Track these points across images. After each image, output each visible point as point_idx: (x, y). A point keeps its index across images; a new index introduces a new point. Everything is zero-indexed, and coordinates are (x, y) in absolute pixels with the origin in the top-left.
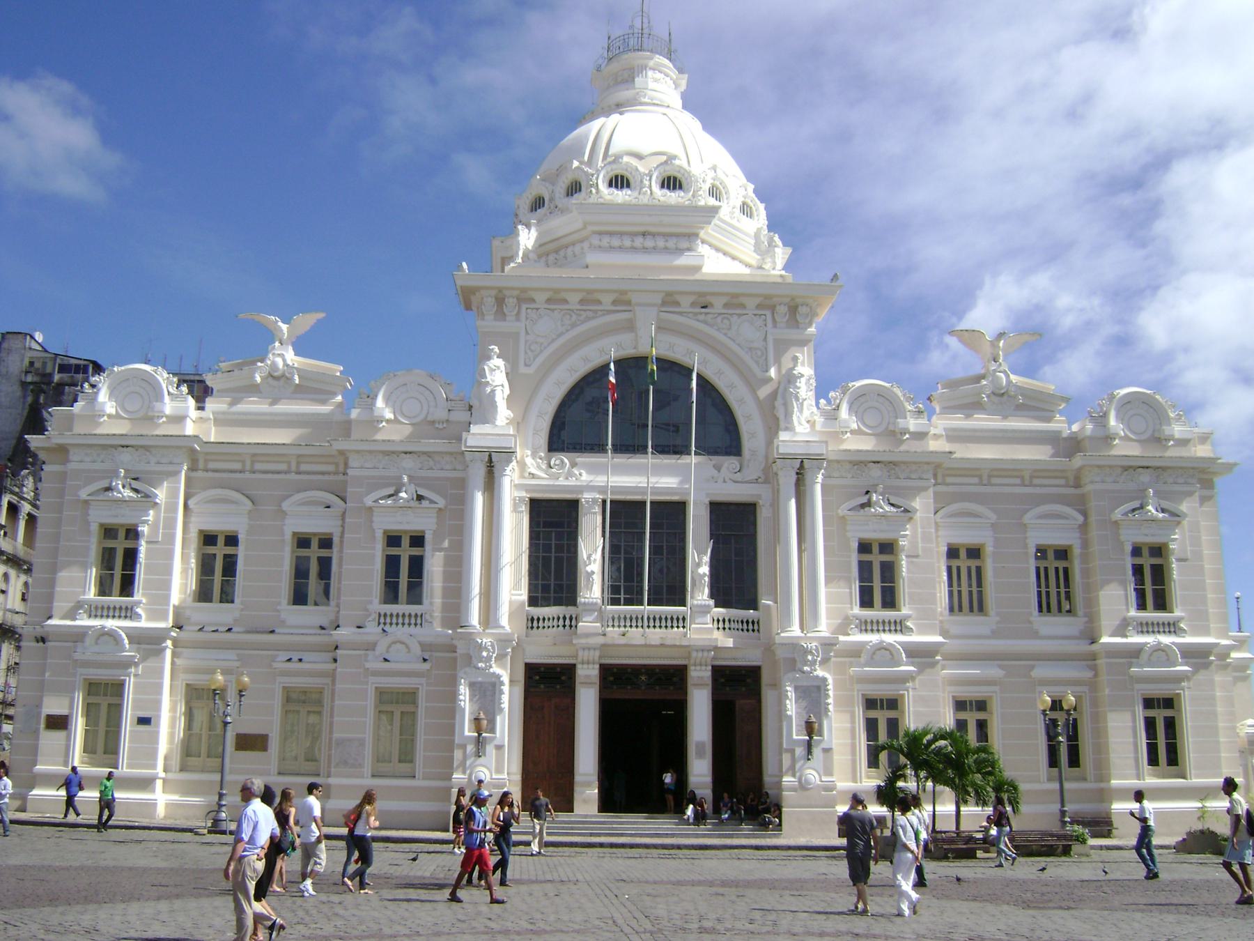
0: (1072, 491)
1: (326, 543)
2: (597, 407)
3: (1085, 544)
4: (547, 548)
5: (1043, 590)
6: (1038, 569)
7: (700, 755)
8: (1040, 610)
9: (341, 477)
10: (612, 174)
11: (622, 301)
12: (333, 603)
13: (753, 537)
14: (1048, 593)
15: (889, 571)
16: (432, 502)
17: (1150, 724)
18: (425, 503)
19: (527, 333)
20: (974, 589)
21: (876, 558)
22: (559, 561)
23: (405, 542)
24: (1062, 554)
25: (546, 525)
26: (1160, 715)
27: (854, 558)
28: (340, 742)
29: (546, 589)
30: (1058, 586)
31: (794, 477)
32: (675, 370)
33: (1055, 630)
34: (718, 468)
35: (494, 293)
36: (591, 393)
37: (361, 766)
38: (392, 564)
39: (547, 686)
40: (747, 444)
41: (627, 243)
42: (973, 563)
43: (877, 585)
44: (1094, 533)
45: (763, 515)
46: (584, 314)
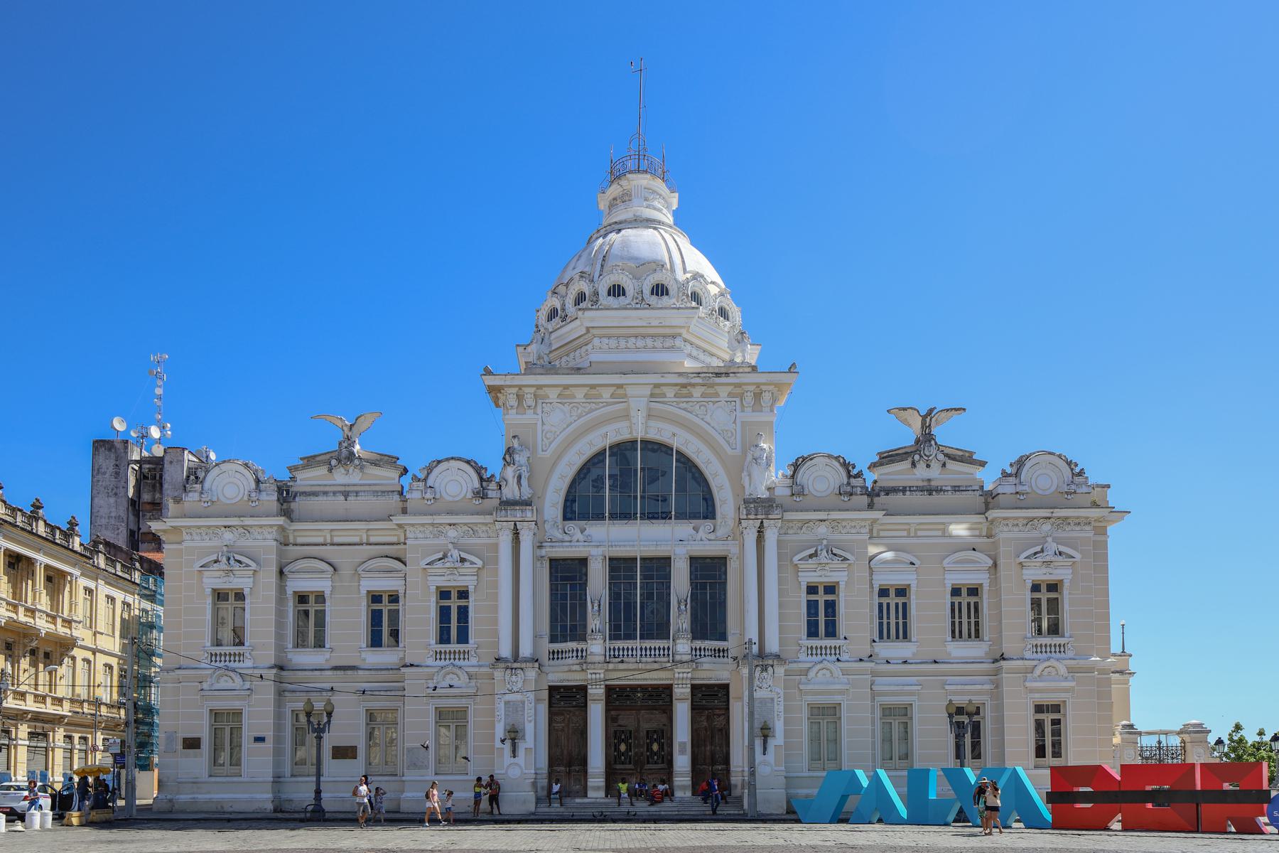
0: (986, 540)
1: (394, 598)
2: (599, 482)
3: (995, 580)
4: (564, 597)
5: (957, 620)
7: (682, 752)
8: (953, 637)
9: (402, 546)
13: (724, 584)
14: (960, 623)
15: (831, 607)
16: (472, 563)
17: (1039, 726)
18: (467, 565)
19: (543, 424)
20: (901, 621)
21: (821, 598)
22: (573, 607)
23: (454, 595)
24: (974, 591)
25: (563, 578)
26: (1048, 718)
27: (804, 598)
29: (564, 628)
30: (969, 617)
34: (696, 529)
35: (515, 390)
36: (595, 472)
37: (427, 767)
38: (444, 613)
39: (565, 702)
41: (623, 343)
42: (900, 600)
43: (822, 618)
45: (732, 567)
46: (589, 406)
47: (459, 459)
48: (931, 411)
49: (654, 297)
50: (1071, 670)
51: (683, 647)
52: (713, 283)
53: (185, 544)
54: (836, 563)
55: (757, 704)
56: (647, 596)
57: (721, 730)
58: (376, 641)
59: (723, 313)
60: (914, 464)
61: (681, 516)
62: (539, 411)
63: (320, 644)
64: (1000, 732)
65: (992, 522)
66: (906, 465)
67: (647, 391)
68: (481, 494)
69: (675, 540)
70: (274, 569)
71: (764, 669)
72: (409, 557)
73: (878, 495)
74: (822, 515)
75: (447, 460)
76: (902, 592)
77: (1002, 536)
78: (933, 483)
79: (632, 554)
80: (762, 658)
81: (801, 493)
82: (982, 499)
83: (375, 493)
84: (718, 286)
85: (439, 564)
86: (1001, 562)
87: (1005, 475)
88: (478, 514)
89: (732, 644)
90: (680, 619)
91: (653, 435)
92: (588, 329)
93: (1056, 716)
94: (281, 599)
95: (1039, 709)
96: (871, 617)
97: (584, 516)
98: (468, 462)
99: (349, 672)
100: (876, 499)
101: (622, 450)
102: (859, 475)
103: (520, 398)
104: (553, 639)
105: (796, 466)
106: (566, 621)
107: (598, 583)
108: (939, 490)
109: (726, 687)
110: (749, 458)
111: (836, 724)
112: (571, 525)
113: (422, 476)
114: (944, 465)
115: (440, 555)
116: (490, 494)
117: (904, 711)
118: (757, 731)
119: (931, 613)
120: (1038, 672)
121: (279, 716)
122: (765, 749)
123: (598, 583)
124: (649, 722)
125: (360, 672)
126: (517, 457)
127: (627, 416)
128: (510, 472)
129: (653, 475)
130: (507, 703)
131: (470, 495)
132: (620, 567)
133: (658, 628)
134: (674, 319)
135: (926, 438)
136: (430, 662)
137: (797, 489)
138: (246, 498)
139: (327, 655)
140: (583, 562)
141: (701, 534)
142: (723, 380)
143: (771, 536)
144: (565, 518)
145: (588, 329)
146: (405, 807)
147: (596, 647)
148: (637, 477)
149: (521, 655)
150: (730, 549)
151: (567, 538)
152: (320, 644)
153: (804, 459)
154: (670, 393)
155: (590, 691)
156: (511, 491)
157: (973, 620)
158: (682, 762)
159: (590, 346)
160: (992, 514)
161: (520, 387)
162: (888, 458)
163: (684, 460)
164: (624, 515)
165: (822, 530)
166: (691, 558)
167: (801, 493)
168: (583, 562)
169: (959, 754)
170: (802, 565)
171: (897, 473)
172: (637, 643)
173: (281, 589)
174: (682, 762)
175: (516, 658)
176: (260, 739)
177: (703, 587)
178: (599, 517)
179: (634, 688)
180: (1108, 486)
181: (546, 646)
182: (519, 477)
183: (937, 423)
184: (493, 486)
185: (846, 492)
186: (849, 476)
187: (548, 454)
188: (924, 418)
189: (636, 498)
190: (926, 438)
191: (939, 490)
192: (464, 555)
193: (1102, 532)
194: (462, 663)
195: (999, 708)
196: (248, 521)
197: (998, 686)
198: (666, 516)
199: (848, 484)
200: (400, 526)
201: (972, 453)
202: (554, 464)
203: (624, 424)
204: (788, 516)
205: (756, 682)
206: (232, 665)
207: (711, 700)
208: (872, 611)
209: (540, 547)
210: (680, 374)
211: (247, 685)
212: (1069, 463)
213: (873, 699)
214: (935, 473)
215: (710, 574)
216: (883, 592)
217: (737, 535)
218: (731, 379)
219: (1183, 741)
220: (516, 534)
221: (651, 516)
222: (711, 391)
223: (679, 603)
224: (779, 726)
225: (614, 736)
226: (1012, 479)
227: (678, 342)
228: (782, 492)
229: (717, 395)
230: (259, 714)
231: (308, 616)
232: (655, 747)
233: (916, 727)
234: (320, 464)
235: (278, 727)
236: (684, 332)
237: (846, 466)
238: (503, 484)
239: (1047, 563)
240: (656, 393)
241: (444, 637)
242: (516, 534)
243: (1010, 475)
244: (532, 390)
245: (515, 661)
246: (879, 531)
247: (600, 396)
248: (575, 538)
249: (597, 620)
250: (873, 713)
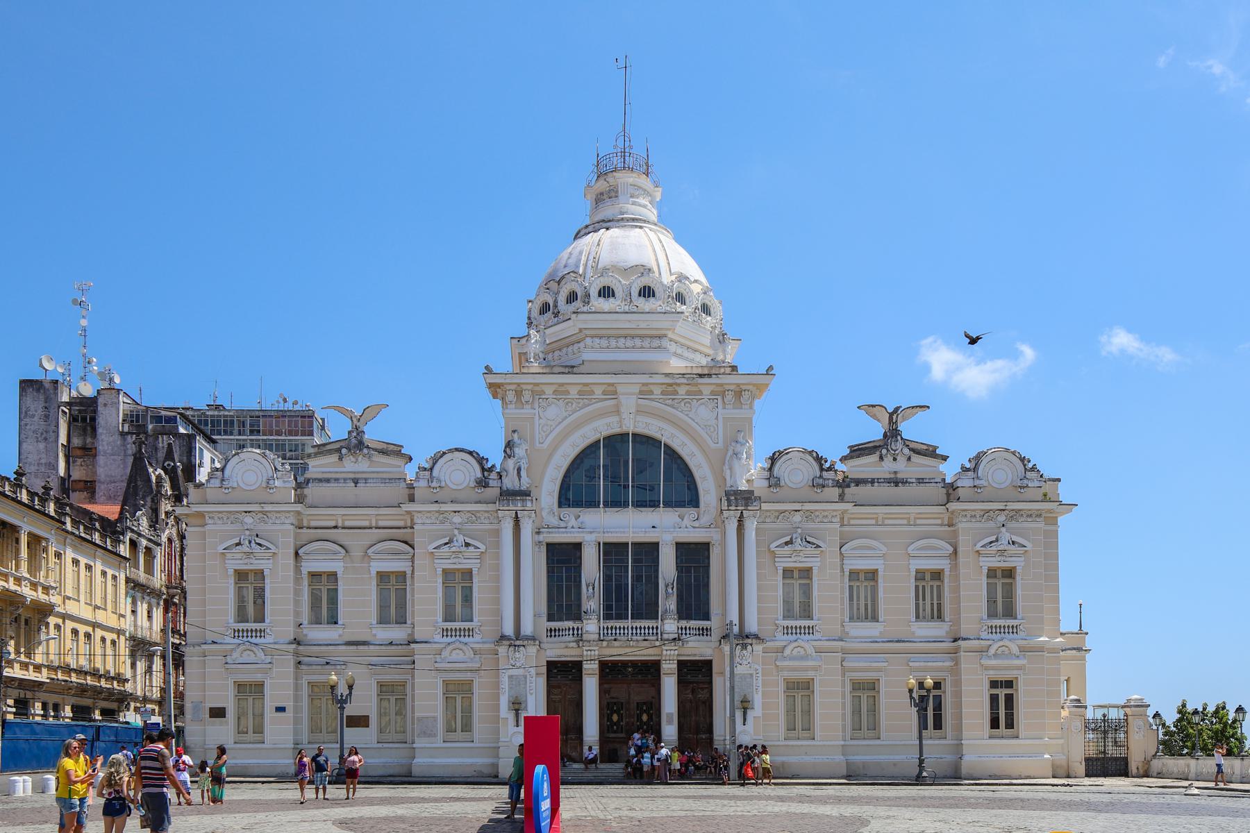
0: (947, 528)
2: (592, 475)
6: (917, 587)
7: (670, 722)
9: (409, 530)
10: (601, 286)
16: (477, 548)
17: (994, 699)
18: (471, 549)
24: (937, 575)
26: (1002, 693)
28: (420, 719)
31: (736, 524)
32: (646, 442)
36: (588, 463)
37: (435, 735)
39: (563, 675)
44: (962, 559)
47: (462, 450)
48: (897, 409)
49: (642, 299)
50: (1023, 650)
51: (671, 626)
52: (696, 281)
53: (207, 527)
54: (810, 550)
55: (737, 679)
56: (637, 578)
57: (704, 703)
58: (383, 620)
59: (706, 309)
60: (881, 458)
61: (668, 504)
62: (536, 406)
63: (334, 621)
64: (958, 705)
65: (953, 513)
66: (874, 458)
67: (636, 389)
68: (483, 483)
69: (664, 527)
70: (292, 551)
71: (744, 647)
72: (417, 541)
73: (848, 486)
74: (797, 506)
75: (450, 451)
76: (872, 575)
77: (960, 525)
78: (899, 476)
79: (624, 540)
80: (745, 638)
81: (777, 485)
82: (944, 491)
83: (384, 481)
84: (701, 283)
85: (446, 548)
86: (961, 549)
87: (965, 469)
88: (480, 502)
89: (714, 623)
90: (668, 602)
91: (641, 430)
92: (581, 330)
93: (1009, 691)
94: (298, 580)
95: (994, 684)
96: (842, 599)
97: (578, 504)
98: (470, 453)
99: (361, 647)
100: (847, 490)
101: (615, 442)
102: (830, 469)
103: (519, 394)
104: (551, 618)
105: (773, 460)
106: (563, 602)
107: (591, 567)
108: (905, 482)
109: (710, 662)
110: (730, 453)
111: (809, 699)
112: (566, 511)
113: (427, 466)
114: (909, 459)
115: (446, 540)
116: (491, 483)
117: (872, 686)
118: (737, 703)
119: (896, 596)
120: (992, 651)
121: (297, 688)
122: (745, 720)
123: (591, 567)
124: (638, 694)
125: (372, 647)
126: (516, 450)
127: (617, 411)
128: (511, 463)
129: (642, 466)
130: (510, 677)
131: (473, 484)
132: (612, 552)
133: (648, 609)
134: (660, 323)
135: (893, 433)
136: (438, 638)
137: (773, 480)
138: (264, 485)
139: (340, 631)
140: (578, 546)
141: (686, 522)
142: (706, 380)
143: (751, 526)
144: (560, 505)
145: (581, 330)
146: (416, 771)
147: (591, 626)
148: (626, 468)
149: (522, 633)
151: (562, 524)
152: (334, 621)
153: (781, 453)
154: (657, 390)
155: (585, 666)
156: (510, 482)
157: (935, 602)
158: (670, 731)
159: (582, 345)
160: (953, 506)
161: (519, 385)
162: (858, 451)
163: (672, 455)
164: (616, 502)
165: (797, 518)
166: (677, 544)
167: (777, 485)
168: (578, 546)
169: (923, 725)
170: (779, 551)
171: (865, 466)
172: (629, 623)
173: (298, 569)
174: (670, 731)
175: (518, 635)
176: (281, 709)
177: (688, 570)
178: (593, 504)
179: (625, 664)
180: (1059, 480)
181: (546, 625)
182: (519, 470)
183: (904, 420)
184: (493, 475)
185: (818, 484)
186: (822, 469)
187: (545, 445)
188: (891, 415)
189: (626, 487)
190: (893, 433)
191: (905, 482)
192: (468, 540)
193: (1054, 522)
194: (467, 639)
195: (958, 683)
196: (268, 508)
197: (957, 663)
198: (654, 504)
199: (821, 477)
200: (408, 512)
201: (935, 448)
202: (551, 456)
203: (614, 419)
204: (765, 506)
205: (737, 659)
206: (254, 640)
207: (696, 675)
208: (843, 593)
209: (538, 533)
210: (667, 375)
211: (268, 659)
212: (1022, 459)
213: (843, 675)
214: (902, 467)
215: (694, 557)
216: (854, 575)
217: (720, 524)
218: (714, 380)
219: (1126, 715)
220: (517, 521)
221: (640, 504)
222: (694, 389)
223: (667, 586)
224: (758, 700)
225: (607, 708)
226: (970, 474)
227: (665, 342)
228: (760, 486)
229: (700, 393)
230: (280, 686)
231: (324, 598)
232: (645, 718)
233: (883, 700)
234: (330, 452)
235: (297, 698)
236: (670, 335)
237: (819, 460)
238: (504, 474)
239: (1002, 552)
240: (645, 392)
242: (517, 521)
243: (968, 470)
244: (529, 387)
245: (517, 639)
246: (850, 519)
247: (593, 393)
248: (570, 525)
249: (592, 601)
250: (843, 686)
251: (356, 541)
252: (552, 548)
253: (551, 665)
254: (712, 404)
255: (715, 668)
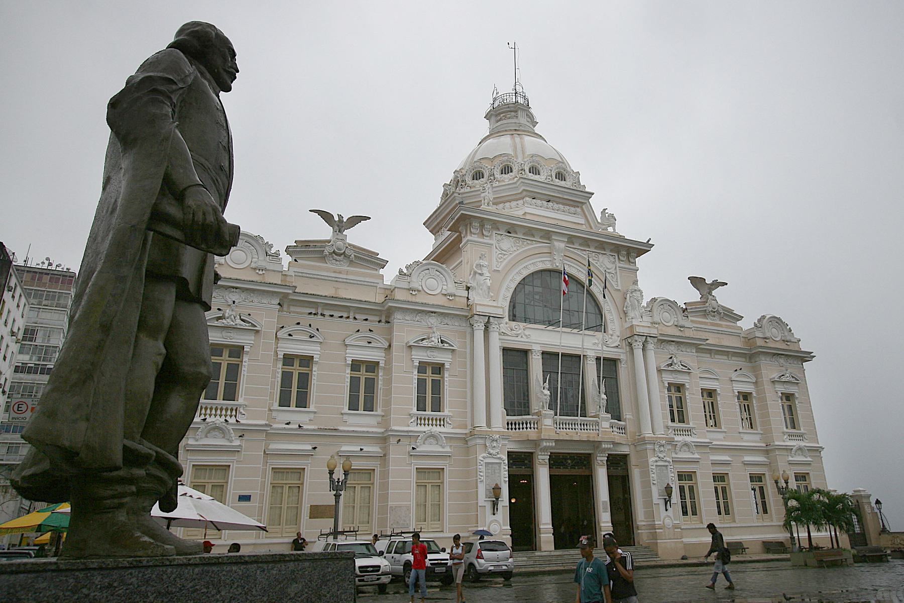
11: (547, 235)
12: (379, 411)
33: (751, 440)
40: (610, 326)
109: (625, 457)
150: (621, 354)
164: (551, 323)
168: (525, 353)
241: (421, 407)
251: (333, 329)
252: (507, 351)
253: (510, 454)
254: (612, 259)
255: (633, 460)
